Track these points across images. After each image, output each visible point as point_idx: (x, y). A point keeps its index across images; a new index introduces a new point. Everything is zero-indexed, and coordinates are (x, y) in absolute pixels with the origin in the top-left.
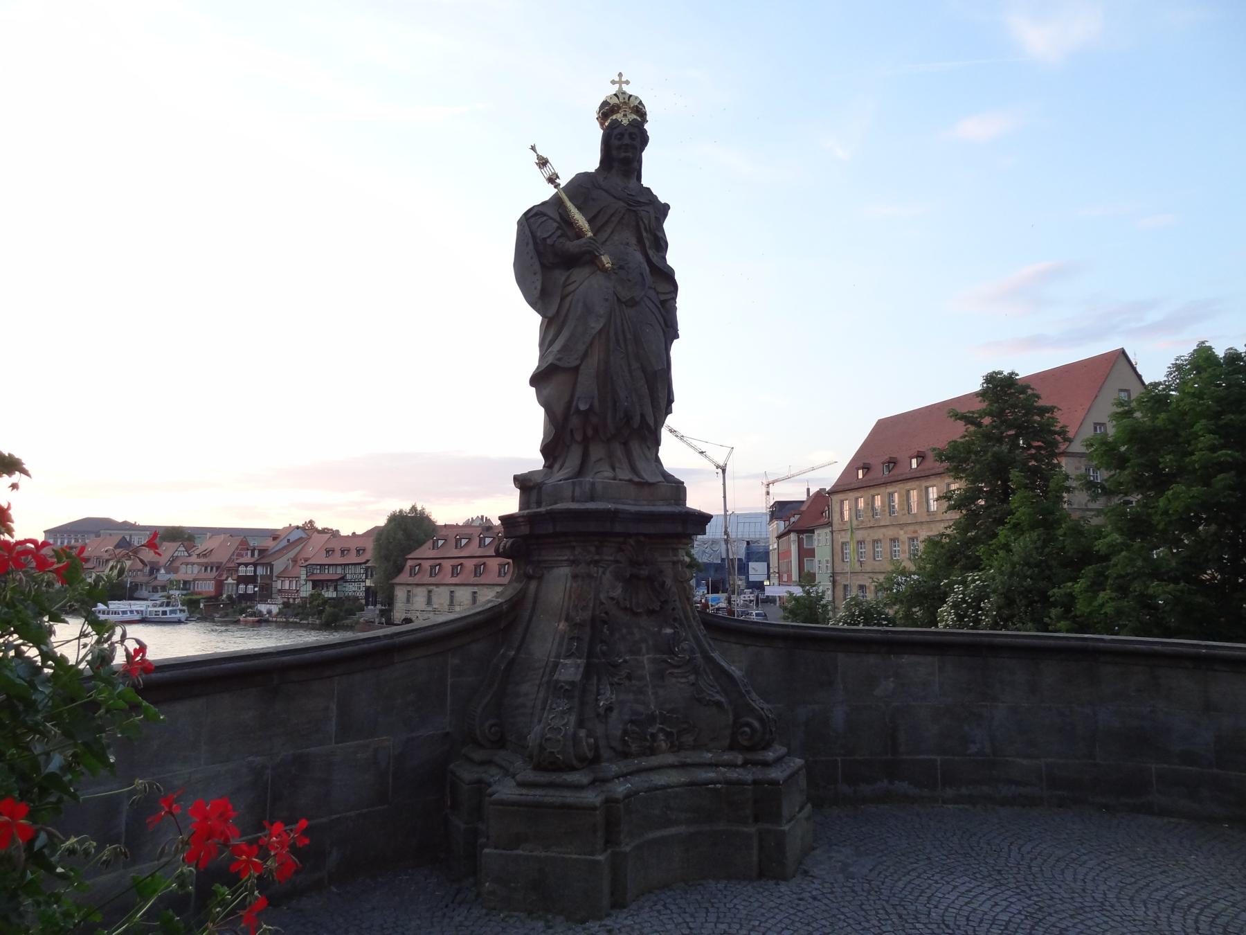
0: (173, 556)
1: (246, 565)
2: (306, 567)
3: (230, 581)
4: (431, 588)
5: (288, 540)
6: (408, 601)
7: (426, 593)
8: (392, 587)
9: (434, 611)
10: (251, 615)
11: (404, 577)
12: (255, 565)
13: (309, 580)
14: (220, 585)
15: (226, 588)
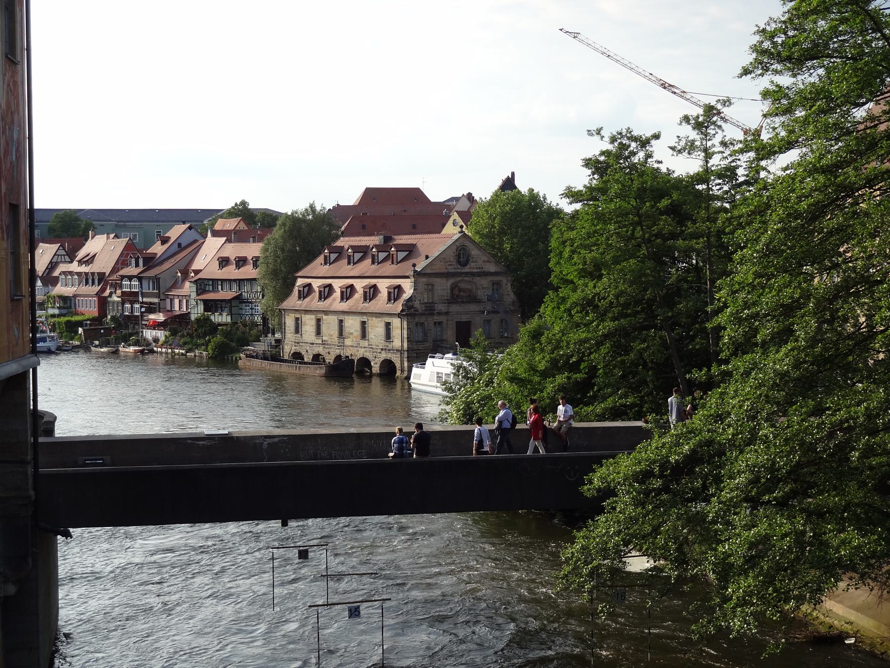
0: (51, 262)
1: (130, 278)
2: (195, 281)
3: (115, 298)
4: (319, 316)
5: (180, 245)
6: (297, 330)
7: (314, 322)
8: (281, 313)
9: (324, 343)
10: (135, 344)
11: (293, 301)
12: (140, 279)
13: (200, 300)
14: (103, 303)
15: (111, 304)
